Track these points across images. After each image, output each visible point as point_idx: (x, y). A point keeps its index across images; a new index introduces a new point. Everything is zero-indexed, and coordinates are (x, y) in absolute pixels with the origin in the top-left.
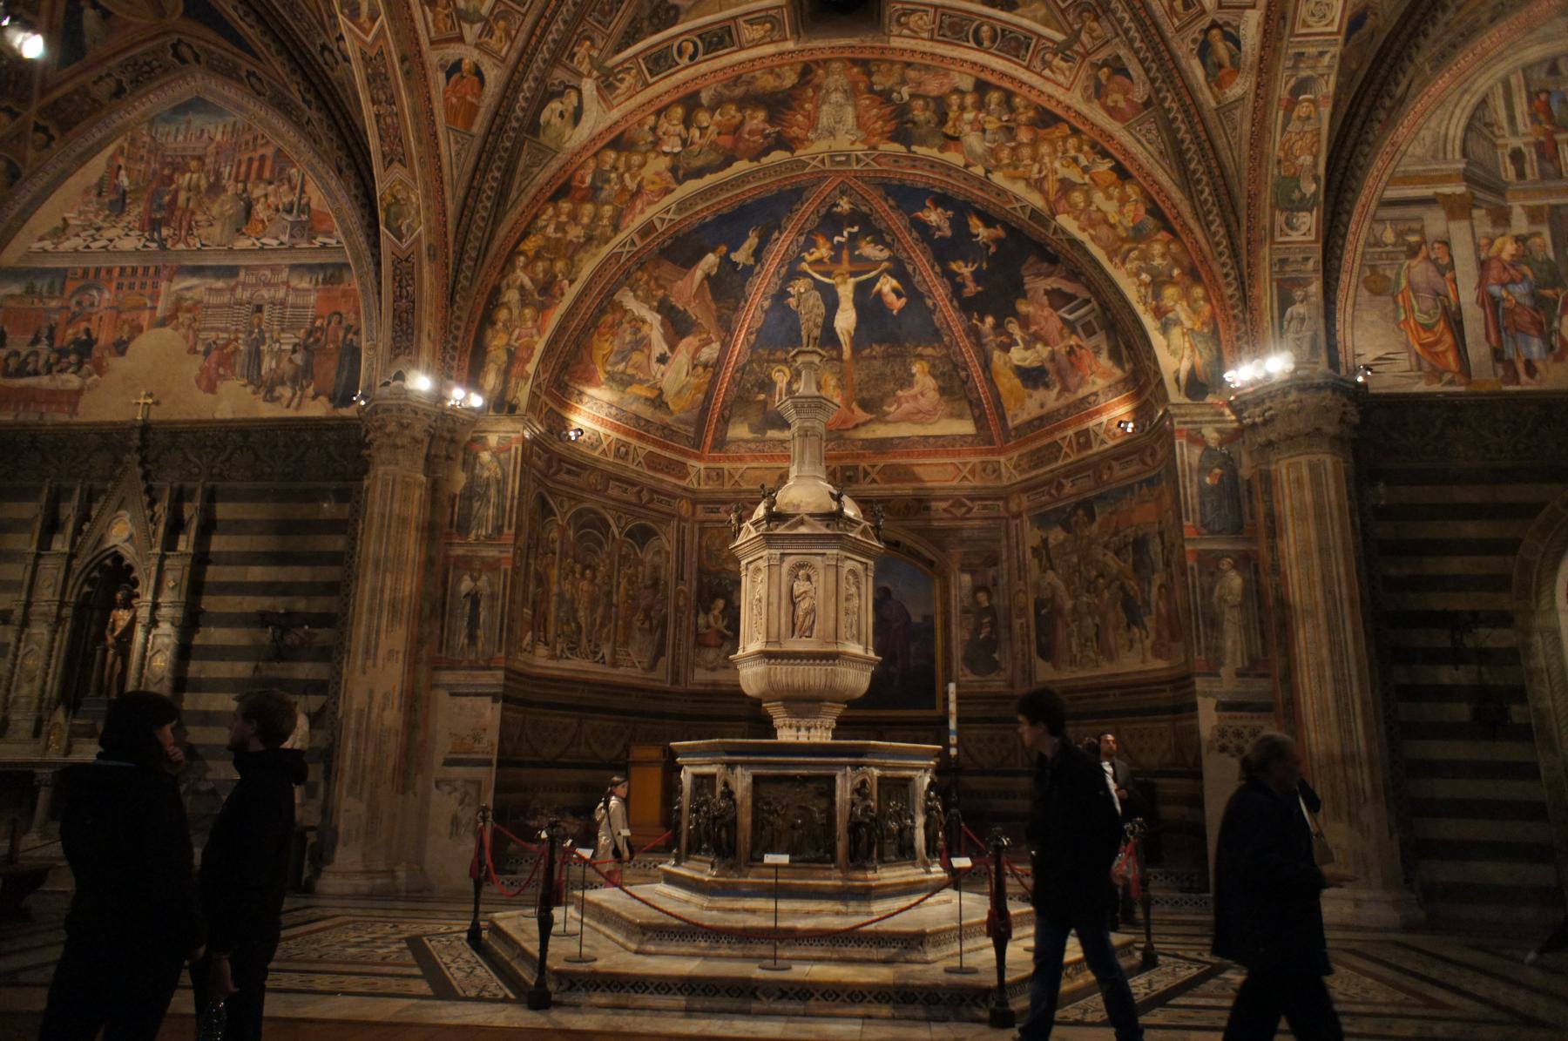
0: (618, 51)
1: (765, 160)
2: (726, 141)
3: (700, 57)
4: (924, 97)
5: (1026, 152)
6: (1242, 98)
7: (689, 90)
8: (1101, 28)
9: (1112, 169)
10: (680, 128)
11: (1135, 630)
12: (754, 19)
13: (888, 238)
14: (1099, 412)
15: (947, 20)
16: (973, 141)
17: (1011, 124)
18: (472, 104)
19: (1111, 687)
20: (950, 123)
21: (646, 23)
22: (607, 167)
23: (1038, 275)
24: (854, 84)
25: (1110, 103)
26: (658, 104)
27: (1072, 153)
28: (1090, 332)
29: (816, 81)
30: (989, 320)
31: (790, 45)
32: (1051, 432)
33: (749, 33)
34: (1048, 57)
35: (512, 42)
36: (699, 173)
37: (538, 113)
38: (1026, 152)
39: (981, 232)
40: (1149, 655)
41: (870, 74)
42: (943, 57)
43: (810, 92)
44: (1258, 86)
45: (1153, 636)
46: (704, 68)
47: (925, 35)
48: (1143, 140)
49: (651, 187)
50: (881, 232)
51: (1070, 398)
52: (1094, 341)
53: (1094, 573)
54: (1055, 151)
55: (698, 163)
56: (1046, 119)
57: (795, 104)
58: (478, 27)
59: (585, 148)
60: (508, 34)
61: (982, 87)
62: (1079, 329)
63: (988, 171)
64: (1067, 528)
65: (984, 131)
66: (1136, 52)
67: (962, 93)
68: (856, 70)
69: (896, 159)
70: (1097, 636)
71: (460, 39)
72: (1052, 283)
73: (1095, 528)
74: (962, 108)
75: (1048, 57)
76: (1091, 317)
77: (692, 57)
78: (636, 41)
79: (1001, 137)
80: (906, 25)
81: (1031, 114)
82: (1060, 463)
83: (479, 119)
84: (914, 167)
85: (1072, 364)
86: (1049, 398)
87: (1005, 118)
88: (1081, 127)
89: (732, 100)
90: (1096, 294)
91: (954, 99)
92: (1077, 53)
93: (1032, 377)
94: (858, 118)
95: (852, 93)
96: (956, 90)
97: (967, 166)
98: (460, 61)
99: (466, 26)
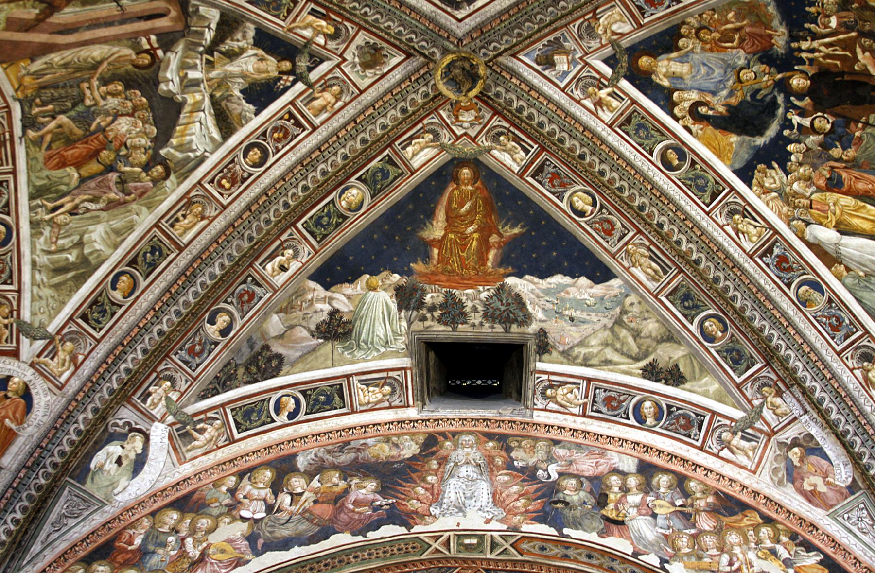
0: (203, 397)
1: (371, 535)
2: (325, 510)
3: (301, 417)
4: (576, 476)
5: (710, 541)
7: (282, 453)
8: (789, 404)
9: (821, 563)
10: (267, 493)
12: (370, 380)
15: (601, 395)
16: (641, 525)
17: (689, 510)
18: (11, 429)
20: (611, 506)
21: (241, 371)
22: (165, 529)
24: (490, 459)
25: (807, 487)
26: (242, 465)
27: (768, 544)
29: (443, 452)
31: (412, 413)
33: (363, 395)
34: (726, 436)
35: (77, 368)
36: (285, 544)
37: (90, 456)
38: (710, 541)
41: (509, 450)
42: (598, 436)
43: (434, 464)
46: (304, 429)
47: (576, 410)
48: (855, 529)
49: (220, 556)
54: (746, 541)
55: (285, 532)
56: (728, 506)
57: (414, 476)
58: (40, 344)
59: (140, 503)
60: (74, 359)
61: (646, 470)
63: (663, 561)
65: (654, 516)
66: (831, 426)
67: (623, 474)
68: (491, 444)
69: (544, 542)
71: (15, 354)
74: (625, 490)
75: (726, 436)
77: (291, 416)
78: (225, 388)
79: (677, 523)
80: (553, 399)
81: (710, 499)
83: (14, 449)
84: (566, 557)
87: (679, 502)
88: (774, 516)
89: (335, 467)
91: (615, 480)
92: (761, 431)
94: (494, 495)
95: (488, 467)
96: (616, 471)
97: (636, 554)
98: (9, 378)
99: (25, 341)
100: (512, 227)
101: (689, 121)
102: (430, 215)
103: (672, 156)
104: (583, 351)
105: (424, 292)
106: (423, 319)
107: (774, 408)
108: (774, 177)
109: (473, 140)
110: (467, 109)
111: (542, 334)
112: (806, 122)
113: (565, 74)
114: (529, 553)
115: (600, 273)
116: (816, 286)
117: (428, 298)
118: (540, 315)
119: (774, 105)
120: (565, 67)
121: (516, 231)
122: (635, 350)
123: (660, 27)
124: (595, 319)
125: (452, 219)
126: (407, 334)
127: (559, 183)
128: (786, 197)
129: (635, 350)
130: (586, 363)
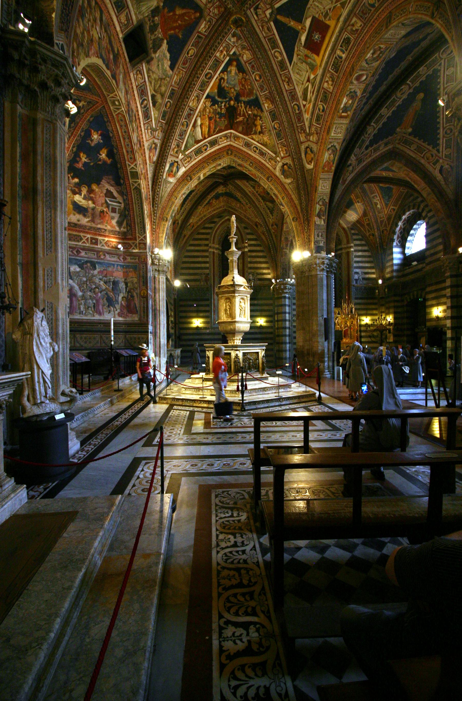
6: (171, 183)
11: (112, 308)
13: (73, 125)
14: (105, 236)
15: (143, 88)
19: (100, 323)
23: (108, 183)
28: (114, 211)
30: (76, 180)
31: (121, 36)
32: (79, 231)
39: (103, 155)
40: (117, 316)
44: (176, 184)
45: (119, 311)
50: (74, 121)
51: (94, 225)
52: (113, 214)
53: (94, 286)
62: (110, 207)
64: (81, 266)
70: (94, 306)
72: (112, 189)
73: (96, 272)
76: (117, 208)
80: (137, 75)
82: (80, 243)
84: (121, 126)
85: (100, 216)
86: (84, 221)
90: (126, 205)
93: (78, 209)
100: (182, 35)
101: (219, 78)
102: (183, 8)
103: (209, 76)
104: (151, 74)
105: (157, 16)
106: (149, 20)
107: (159, 133)
108: (209, 104)
109: (209, 15)
110: (219, 11)
111: (152, 59)
112: (223, 107)
113: (230, 41)
114: (118, 117)
115: (172, 67)
116: (187, 126)
117: (156, 18)
118: (157, 55)
119: (226, 98)
120: (232, 40)
121: (180, 36)
122: (156, 88)
123: (245, 68)
124: (161, 71)
125: (183, 15)
126: (144, 18)
127: (196, 44)
128: (204, 109)
129: (156, 88)
130: (149, 77)
